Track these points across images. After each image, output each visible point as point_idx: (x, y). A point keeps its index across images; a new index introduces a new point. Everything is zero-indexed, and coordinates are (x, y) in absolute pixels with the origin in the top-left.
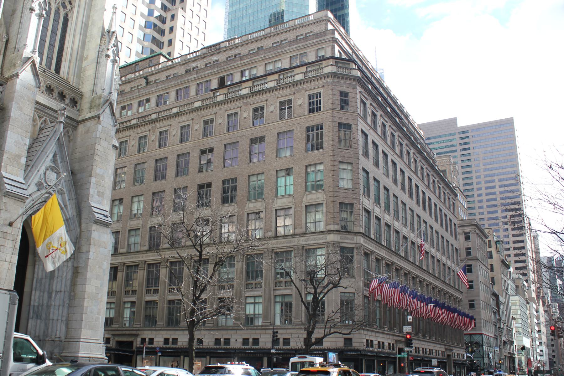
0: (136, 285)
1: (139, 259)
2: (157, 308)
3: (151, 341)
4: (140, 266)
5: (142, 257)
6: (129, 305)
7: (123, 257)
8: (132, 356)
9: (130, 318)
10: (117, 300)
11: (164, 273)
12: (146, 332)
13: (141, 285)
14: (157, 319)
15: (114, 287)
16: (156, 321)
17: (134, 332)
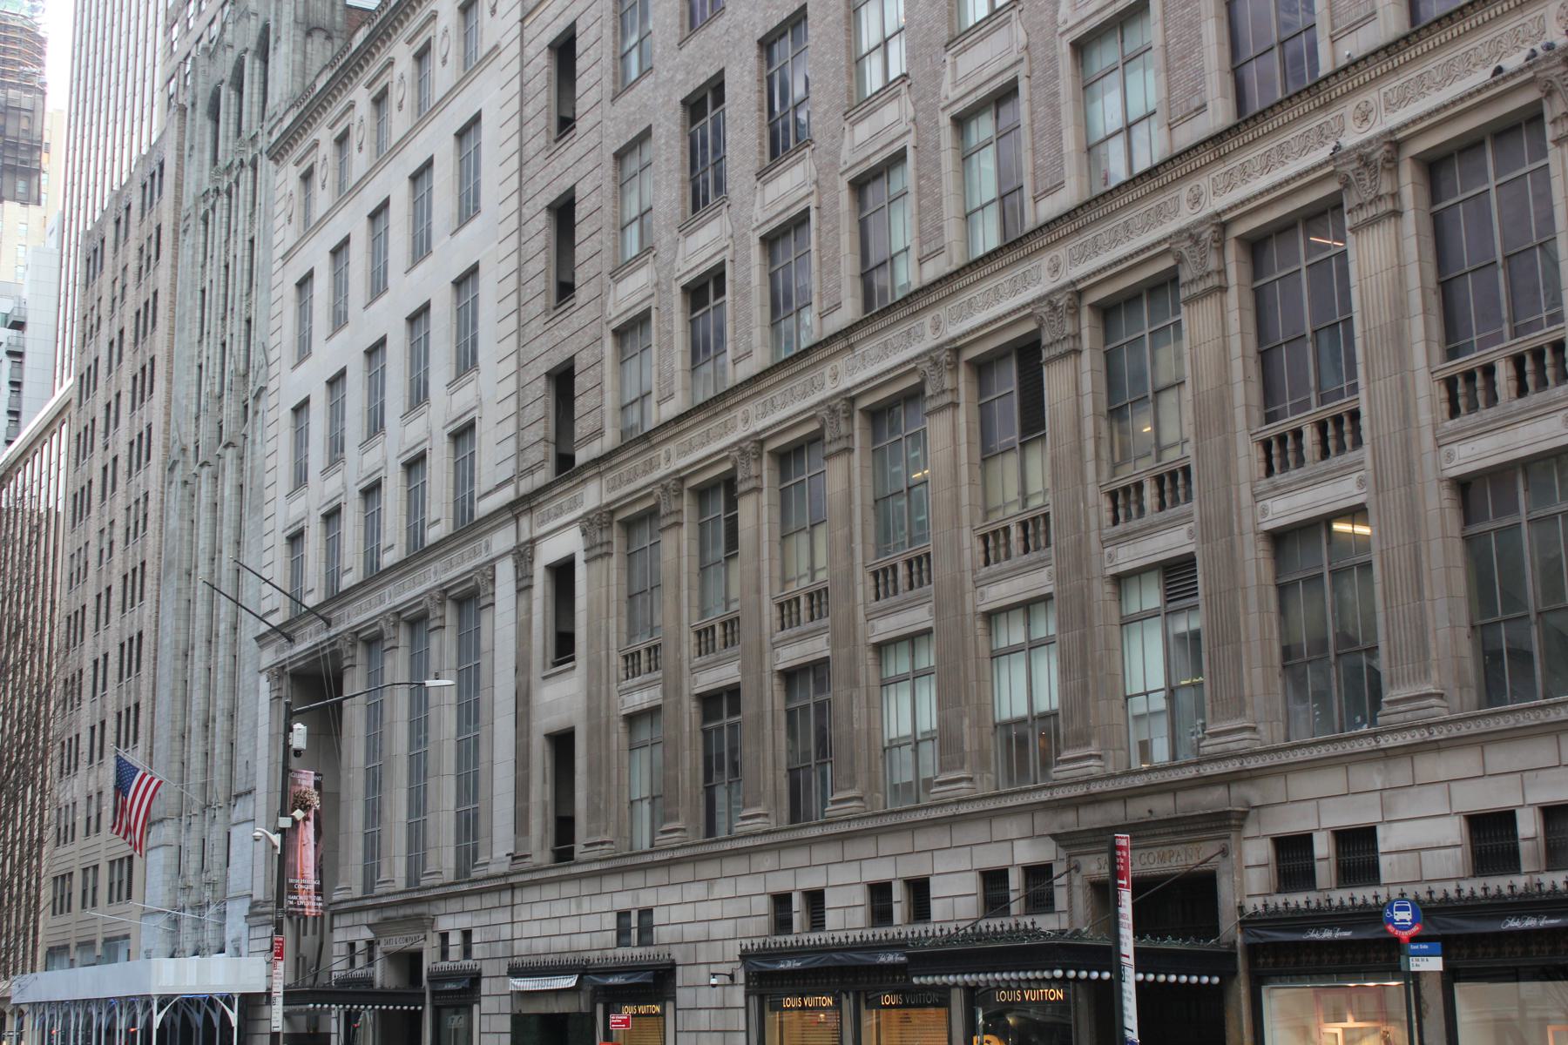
0: (1172, 427)
1: (1170, 227)
2: (1367, 567)
3: (1357, 847)
4: (1185, 275)
5: (1196, 201)
6: (1150, 596)
7: (1061, 252)
8: (1216, 998)
9: (1172, 692)
10: (1060, 578)
11: (1383, 262)
12: (1304, 785)
13: (1212, 416)
14: (1382, 663)
15: (1036, 483)
16: (1375, 675)
17: (1213, 799)
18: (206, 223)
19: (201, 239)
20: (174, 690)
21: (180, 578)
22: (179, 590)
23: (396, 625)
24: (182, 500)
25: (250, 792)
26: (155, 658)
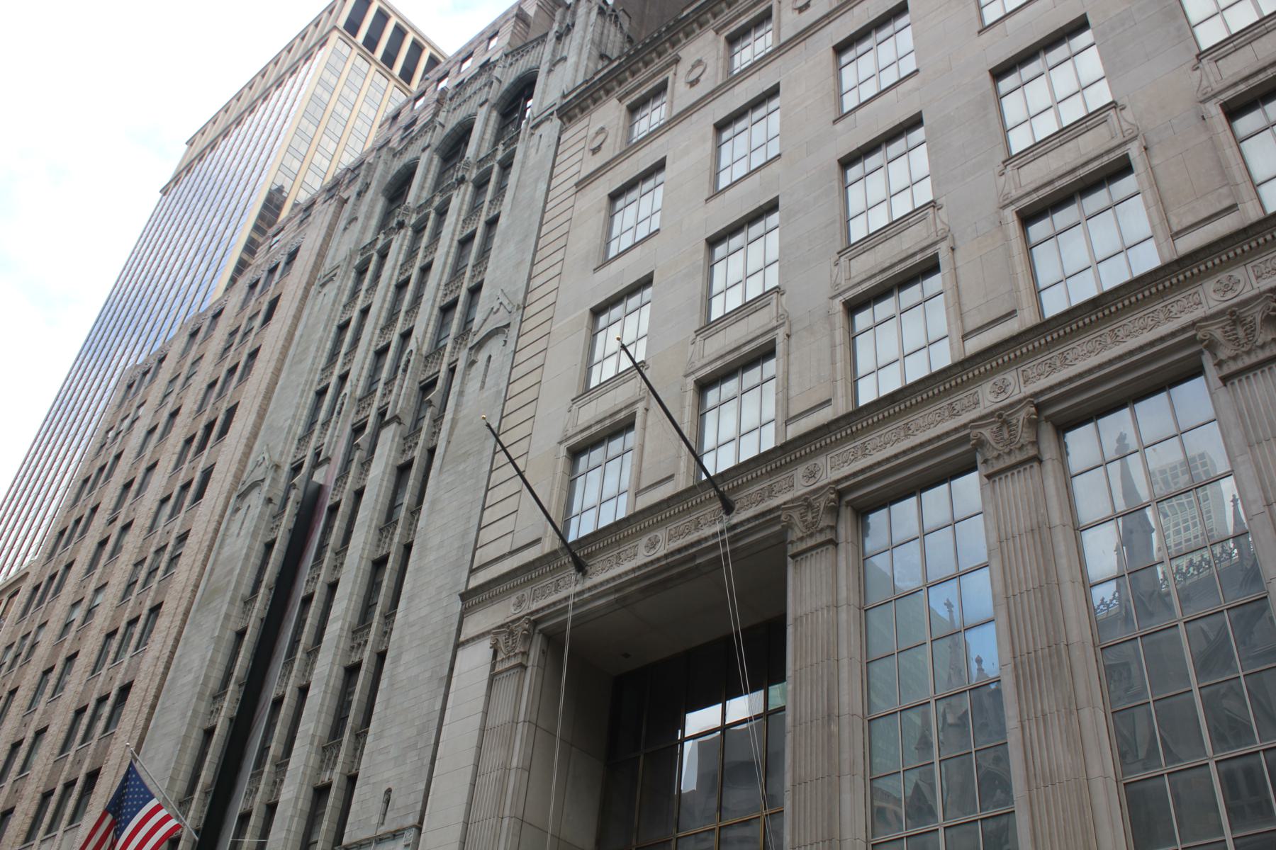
18: (361, 271)
19: (350, 284)
20: (187, 737)
21: (232, 602)
22: (227, 617)
23: (1033, 424)
24: (262, 514)
25: (395, 835)
26: (153, 707)
